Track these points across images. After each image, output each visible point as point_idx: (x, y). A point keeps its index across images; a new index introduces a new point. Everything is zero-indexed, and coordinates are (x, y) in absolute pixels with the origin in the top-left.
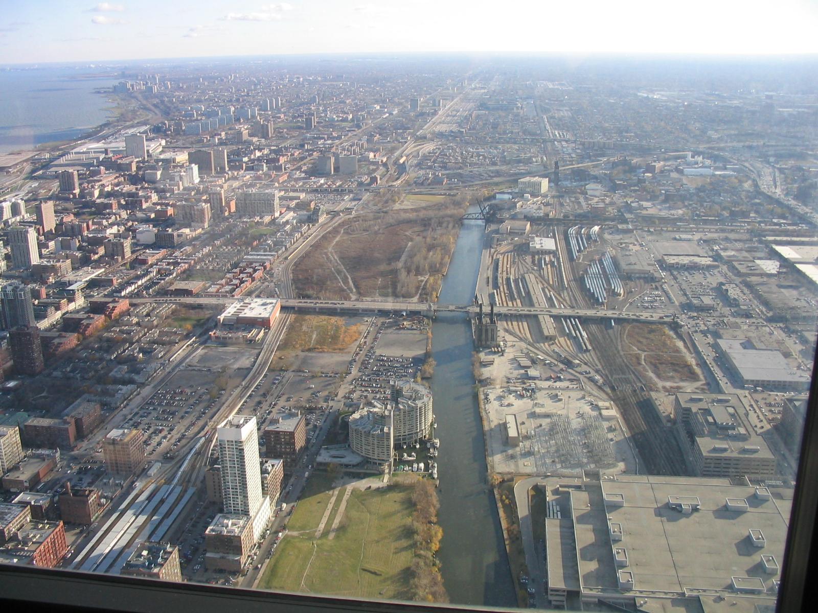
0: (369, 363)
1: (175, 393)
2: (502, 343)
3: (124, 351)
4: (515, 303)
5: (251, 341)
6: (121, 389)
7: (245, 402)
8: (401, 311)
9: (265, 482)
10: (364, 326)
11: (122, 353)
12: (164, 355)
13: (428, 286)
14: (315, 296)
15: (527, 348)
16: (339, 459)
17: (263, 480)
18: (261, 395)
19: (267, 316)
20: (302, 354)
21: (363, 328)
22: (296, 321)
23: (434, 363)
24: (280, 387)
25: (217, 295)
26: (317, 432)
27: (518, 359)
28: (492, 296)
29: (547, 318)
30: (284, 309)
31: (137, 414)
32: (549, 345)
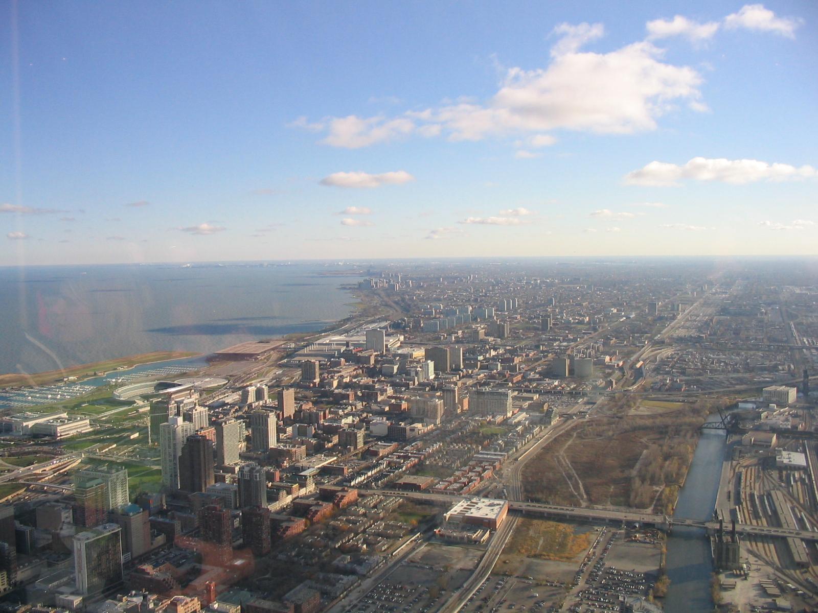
0: (597, 575)
1: (395, 588)
2: (745, 566)
3: (349, 541)
4: (760, 522)
5: (476, 542)
6: (342, 579)
10: (597, 535)
11: (346, 543)
12: (388, 548)
13: (663, 495)
14: (544, 500)
15: (774, 574)
18: (482, 600)
19: (493, 517)
20: (527, 560)
21: (593, 537)
22: (523, 524)
23: (668, 581)
24: (502, 592)
25: (444, 492)
27: (764, 586)
28: (733, 513)
29: (798, 541)
30: (511, 511)
31: (355, 606)
32: (802, 573)
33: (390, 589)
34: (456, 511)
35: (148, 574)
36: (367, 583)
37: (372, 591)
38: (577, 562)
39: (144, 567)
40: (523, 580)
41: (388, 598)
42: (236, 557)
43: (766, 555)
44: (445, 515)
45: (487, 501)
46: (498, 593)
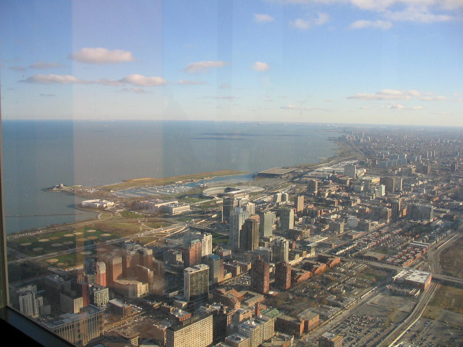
1: (362, 317)
3: (335, 287)
5: (411, 296)
6: (331, 309)
7: (406, 333)
11: (333, 288)
12: (358, 293)
14: (455, 275)
19: (423, 282)
20: (445, 311)
25: (392, 263)
30: (433, 279)
31: (339, 325)
33: (359, 318)
34: (399, 276)
35: (223, 294)
36: (345, 313)
37: (349, 318)
39: (221, 290)
41: (358, 323)
42: (270, 289)
44: (393, 277)
45: (419, 272)
46: (426, 329)
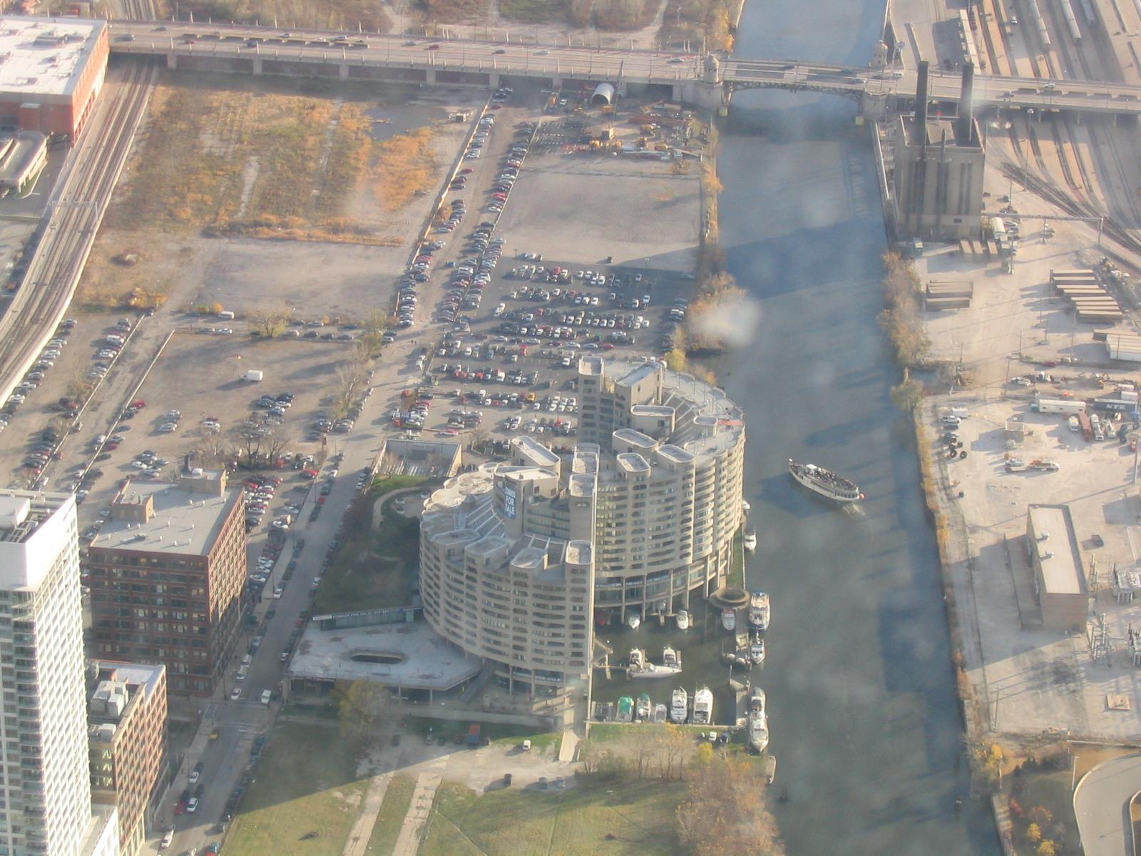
0: (475, 289)
2: (999, 224)
8: (595, 83)
9: (106, 754)
14: (244, 11)
15: (1099, 247)
16: (379, 668)
17: (97, 743)
18: (52, 408)
20: (207, 249)
21: (446, 147)
22: (173, 112)
24: (125, 375)
26: (286, 557)
27: (1068, 289)
28: (948, 34)
30: (118, 60)
38: (394, 244)
40: (200, 323)
43: (1070, 181)
46: (109, 380)
